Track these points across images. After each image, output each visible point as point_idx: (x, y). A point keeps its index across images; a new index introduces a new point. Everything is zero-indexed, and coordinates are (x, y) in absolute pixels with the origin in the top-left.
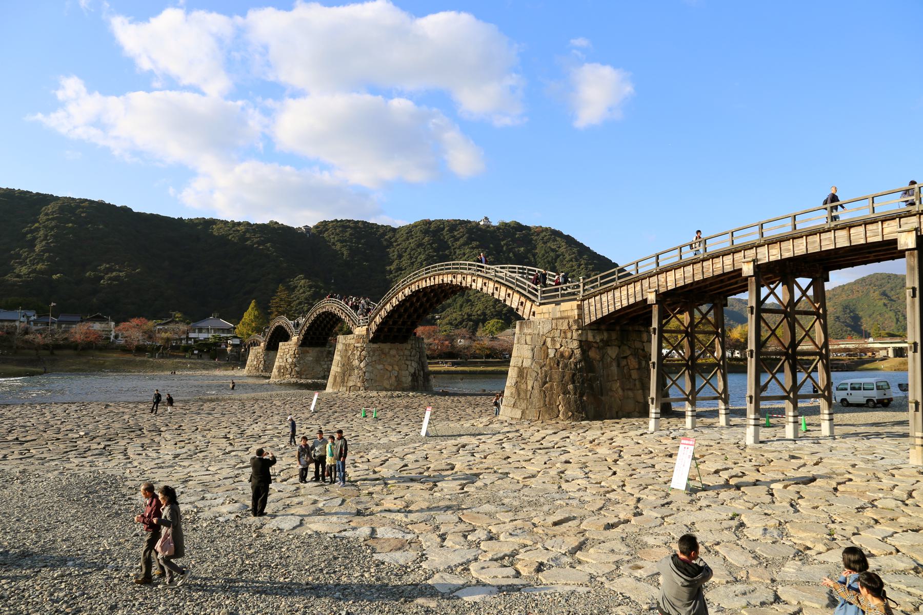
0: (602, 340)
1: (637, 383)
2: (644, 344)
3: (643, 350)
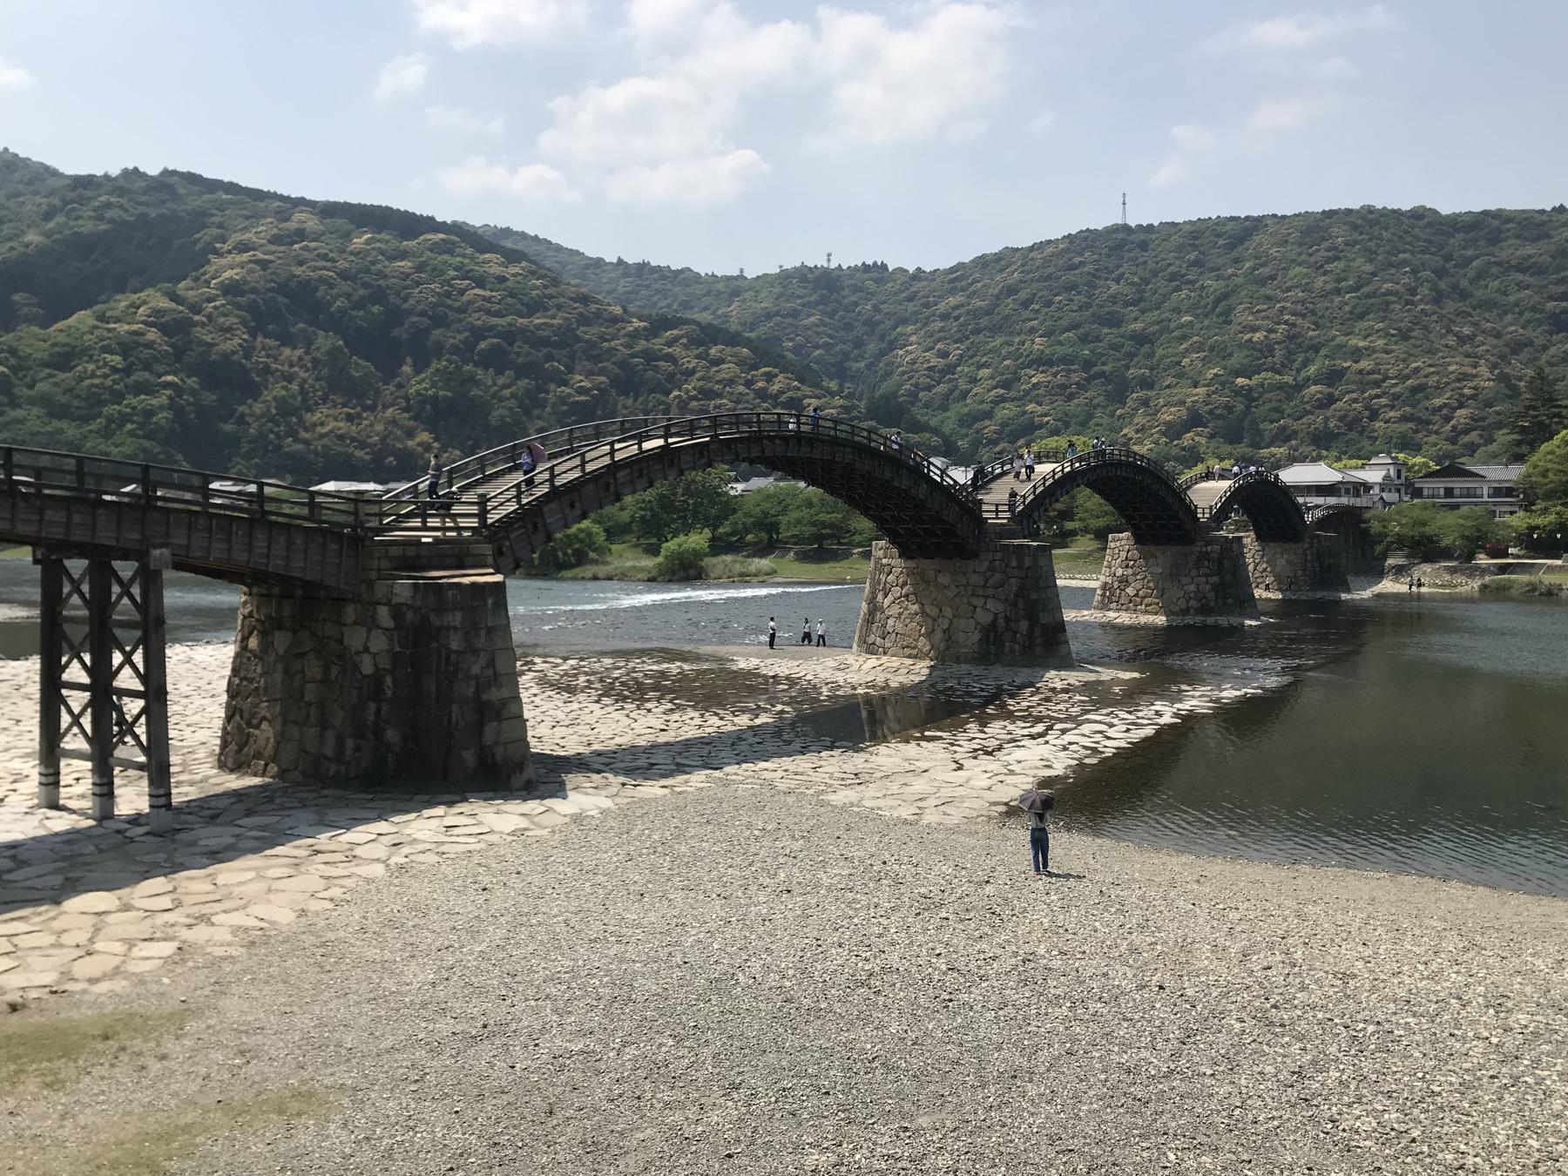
0: (269, 617)
1: (313, 711)
2: (345, 629)
3: (341, 642)
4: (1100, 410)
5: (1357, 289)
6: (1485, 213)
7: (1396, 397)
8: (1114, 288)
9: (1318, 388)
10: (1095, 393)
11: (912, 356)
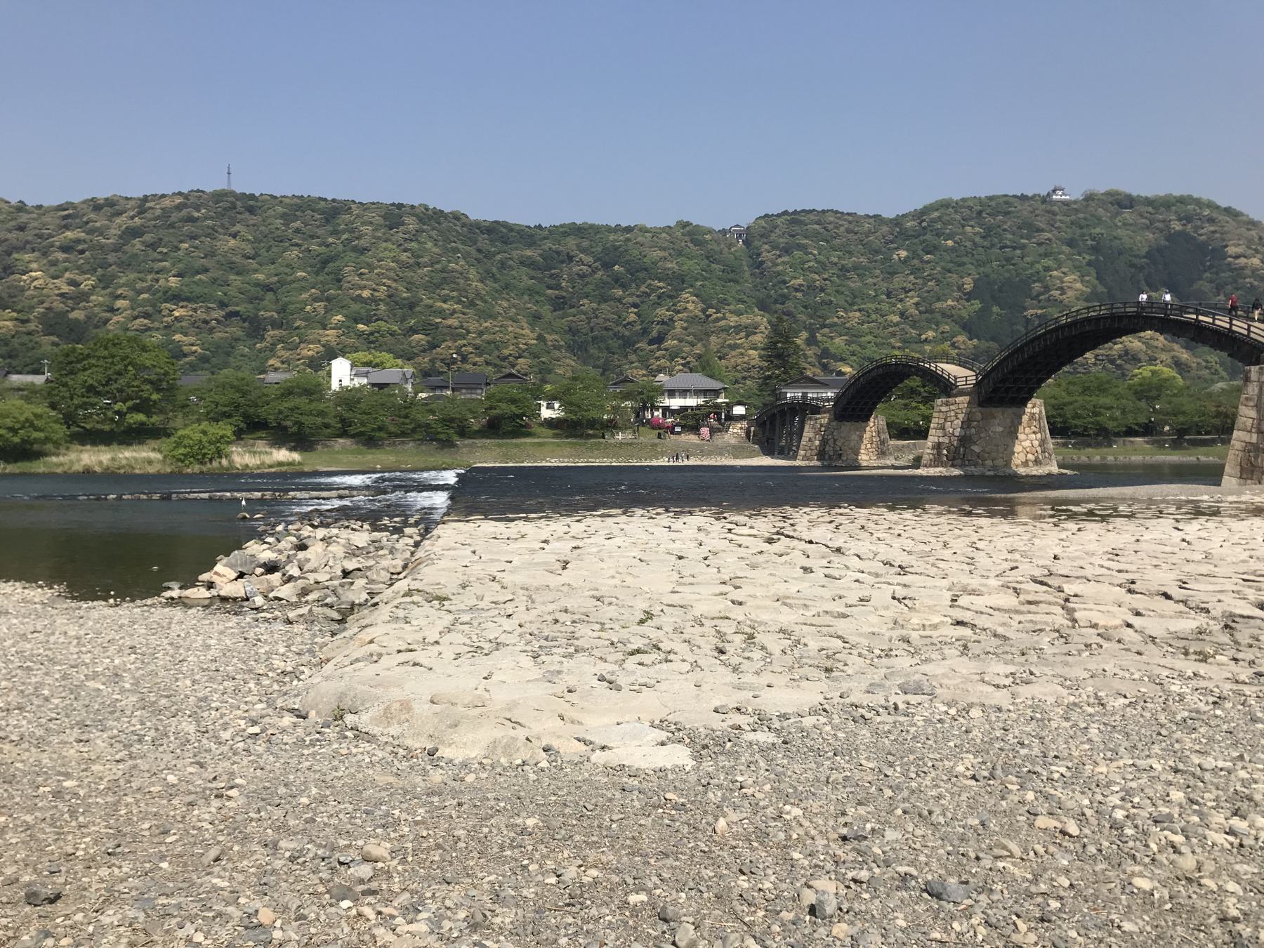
4: (241, 343)
5: (432, 265)
6: (496, 222)
7: (477, 347)
8: (232, 242)
9: (420, 336)
10: (235, 330)
11: (41, 281)
